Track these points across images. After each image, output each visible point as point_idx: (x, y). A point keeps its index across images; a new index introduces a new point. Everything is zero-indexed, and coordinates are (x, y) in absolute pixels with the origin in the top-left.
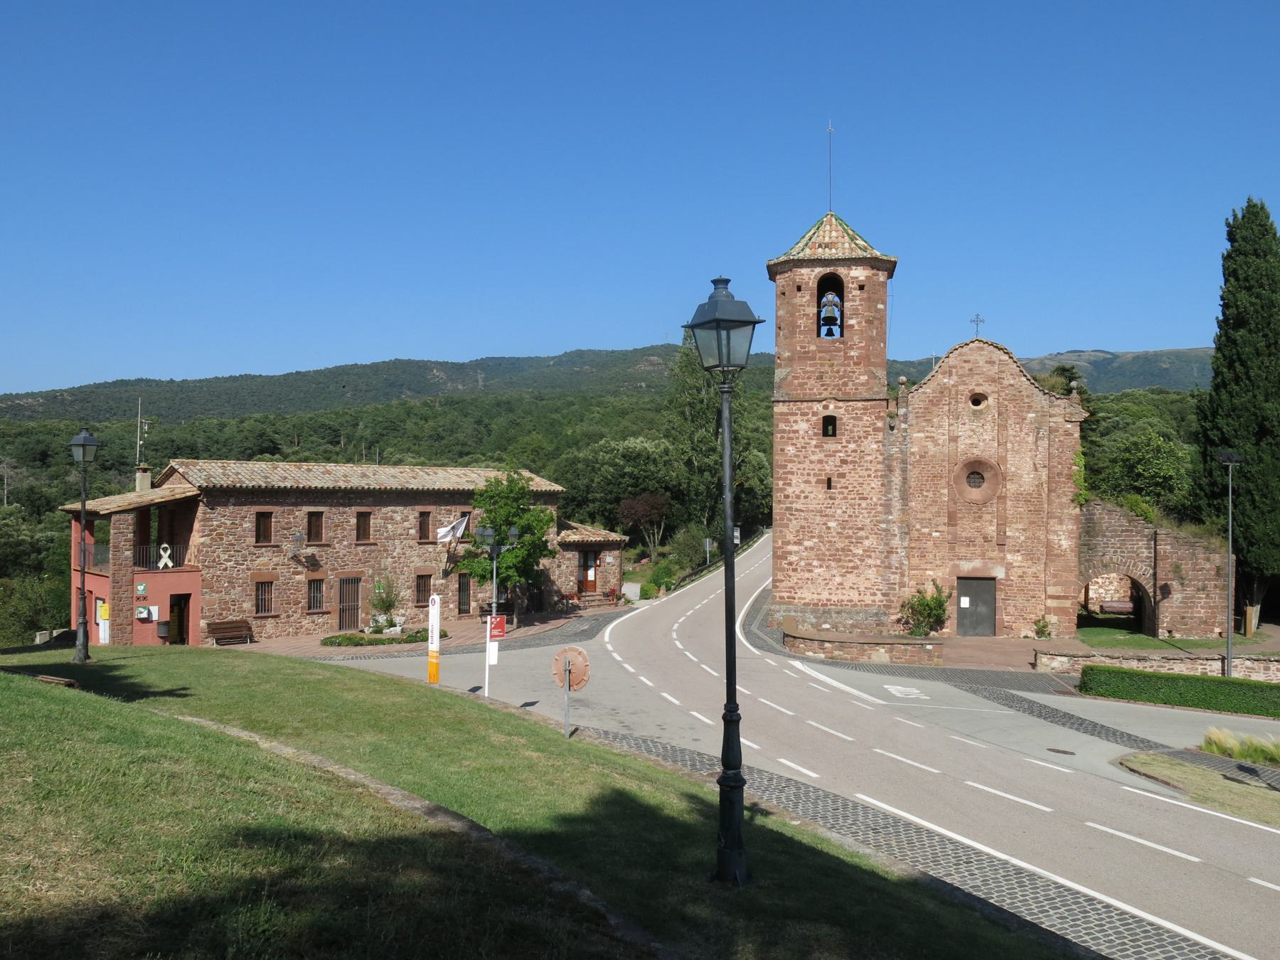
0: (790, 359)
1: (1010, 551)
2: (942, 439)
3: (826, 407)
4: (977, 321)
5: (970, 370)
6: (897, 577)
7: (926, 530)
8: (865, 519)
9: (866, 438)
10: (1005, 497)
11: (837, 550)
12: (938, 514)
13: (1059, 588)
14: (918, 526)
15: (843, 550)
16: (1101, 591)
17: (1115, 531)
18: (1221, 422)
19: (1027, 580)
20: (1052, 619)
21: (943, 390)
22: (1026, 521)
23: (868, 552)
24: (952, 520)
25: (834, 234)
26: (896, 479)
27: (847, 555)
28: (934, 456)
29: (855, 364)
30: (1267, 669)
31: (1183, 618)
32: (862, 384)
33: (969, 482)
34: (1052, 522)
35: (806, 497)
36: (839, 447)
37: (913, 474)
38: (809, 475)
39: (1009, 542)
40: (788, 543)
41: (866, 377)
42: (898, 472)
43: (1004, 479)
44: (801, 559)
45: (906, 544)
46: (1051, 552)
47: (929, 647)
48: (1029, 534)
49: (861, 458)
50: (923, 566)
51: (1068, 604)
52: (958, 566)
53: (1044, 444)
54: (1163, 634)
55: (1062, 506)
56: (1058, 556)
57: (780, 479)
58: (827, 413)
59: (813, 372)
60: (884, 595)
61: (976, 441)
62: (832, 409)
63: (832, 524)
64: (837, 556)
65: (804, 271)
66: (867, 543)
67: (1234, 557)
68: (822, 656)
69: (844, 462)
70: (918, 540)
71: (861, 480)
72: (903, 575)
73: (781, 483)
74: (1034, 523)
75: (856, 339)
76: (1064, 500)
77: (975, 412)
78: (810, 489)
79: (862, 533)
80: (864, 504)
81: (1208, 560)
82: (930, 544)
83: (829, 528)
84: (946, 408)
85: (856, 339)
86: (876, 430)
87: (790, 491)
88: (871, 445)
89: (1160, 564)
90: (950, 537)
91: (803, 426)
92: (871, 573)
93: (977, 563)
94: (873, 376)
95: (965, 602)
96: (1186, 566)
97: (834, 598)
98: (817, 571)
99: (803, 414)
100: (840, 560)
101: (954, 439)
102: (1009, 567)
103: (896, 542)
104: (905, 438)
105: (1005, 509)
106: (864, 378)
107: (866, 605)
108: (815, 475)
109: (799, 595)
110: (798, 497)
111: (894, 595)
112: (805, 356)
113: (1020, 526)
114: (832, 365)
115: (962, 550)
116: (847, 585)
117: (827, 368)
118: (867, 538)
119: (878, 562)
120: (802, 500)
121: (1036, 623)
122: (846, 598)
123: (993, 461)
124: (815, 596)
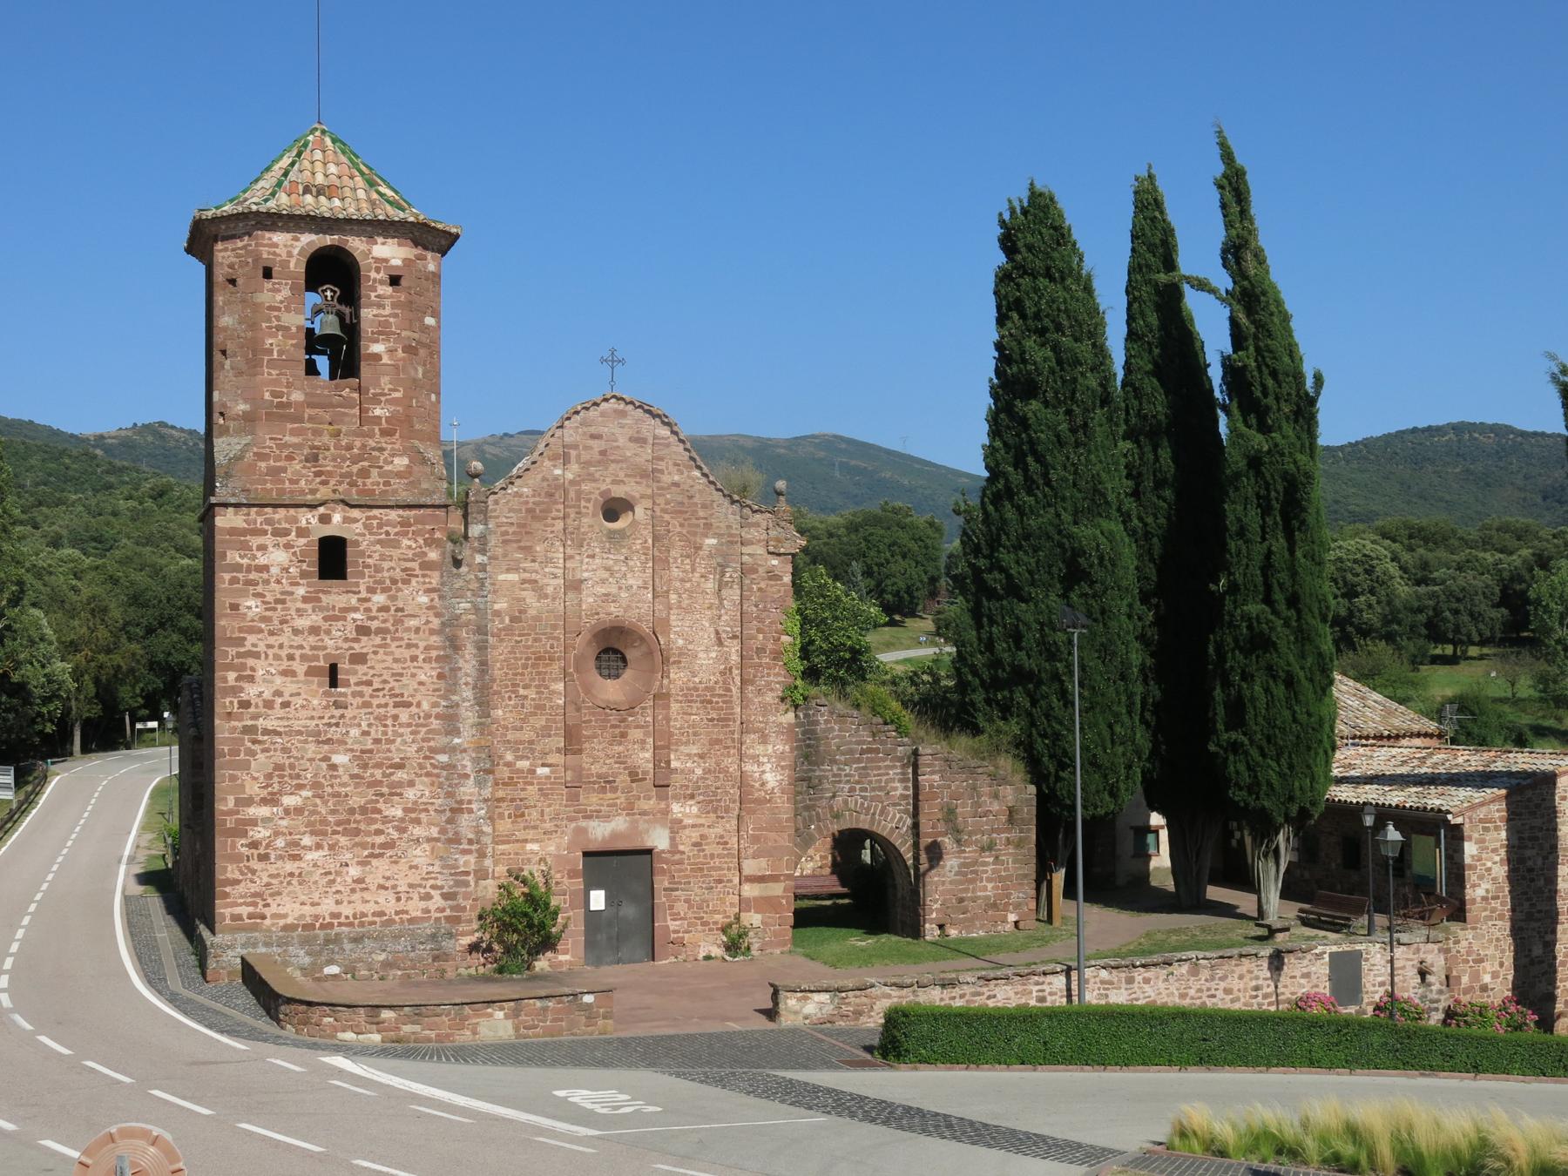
0: (249, 419)
1: (676, 798)
2: (553, 585)
3: (325, 519)
4: (613, 361)
5: (603, 453)
6: (472, 859)
7: (523, 764)
8: (406, 747)
9: (406, 582)
10: (667, 696)
11: (352, 811)
12: (545, 732)
13: (763, 862)
14: (509, 757)
17: (851, 752)
18: (1006, 557)
19: (709, 849)
20: (753, 919)
21: (554, 491)
24: (573, 741)
25: (332, 169)
26: (467, 664)
27: (374, 821)
28: (537, 618)
29: (384, 433)
30: (1130, 981)
31: (961, 900)
32: (399, 475)
33: (599, 668)
34: (748, 739)
35: (286, 705)
37: (499, 652)
38: (291, 657)
39: (677, 781)
40: (249, 802)
41: (405, 461)
42: (469, 651)
43: (665, 661)
44: (277, 834)
45: (487, 793)
46: (747, 796)
47: (588, 999)
48: (710, 763)
49: (398, 622)
50: (520, 835)
51: (777, 889)
52: (584, 831)
53: (733, 594)
54: (931, 931)
55: (765, 709)
57: (230, 667)
58: (328, 531)
59: (294, 446)
60: (445, 896)
61: (614, 590)
62: (338, 523)
63: (340, 759)
64: (351, 824)
65: (279, 238)
66: (411, 794)
67: (1032, 789)
68: (377, 1038)
69: (363, 631)
70: (510, 783)
71: (397, 667)
72: (482, 855)
73: (231, 676)
74: (718, 741)
75: (385, 382)
76: (770, 698)
77: (611, 534)
78: (293, 688)
79: (401, 775)
80: (404, 716)
81: (996, 796)
82: (532, 790)
83: (333, 767)
84: (559, 525)
85: (385, 382)
86: (427, 566)
87: (251, 691)
88: (417, 598)
89: (925, 808)
91: (277, 557)
92: (420, 855)
93: (619, 823)
94: (419, 458)
95: (598, 900)
96: (964, 809)
97: (347, 910)
98: (311, 856)
99: (276, 533)
100: (357, 832)
101: (574, 586)
102: (676, 827)
103: (468, 789)
104: (482, 582)
105: (668, 719)
106: (401, 462)
107: (412, 921)
108: (304, 658)
109: (274, 909)
110: (269, 704)
111: (466, 896)
112: (281, 413)
113: (694, 750)
114: (337, 434)
115: (592, 800)
116: (373, 880)
117: (326, 439)
118: (411, 784)
119: (434, 832)
120: (278, 711)
121: (724, 930)
122: (370, 908)
123: (646, 628)
124: (308, 910)
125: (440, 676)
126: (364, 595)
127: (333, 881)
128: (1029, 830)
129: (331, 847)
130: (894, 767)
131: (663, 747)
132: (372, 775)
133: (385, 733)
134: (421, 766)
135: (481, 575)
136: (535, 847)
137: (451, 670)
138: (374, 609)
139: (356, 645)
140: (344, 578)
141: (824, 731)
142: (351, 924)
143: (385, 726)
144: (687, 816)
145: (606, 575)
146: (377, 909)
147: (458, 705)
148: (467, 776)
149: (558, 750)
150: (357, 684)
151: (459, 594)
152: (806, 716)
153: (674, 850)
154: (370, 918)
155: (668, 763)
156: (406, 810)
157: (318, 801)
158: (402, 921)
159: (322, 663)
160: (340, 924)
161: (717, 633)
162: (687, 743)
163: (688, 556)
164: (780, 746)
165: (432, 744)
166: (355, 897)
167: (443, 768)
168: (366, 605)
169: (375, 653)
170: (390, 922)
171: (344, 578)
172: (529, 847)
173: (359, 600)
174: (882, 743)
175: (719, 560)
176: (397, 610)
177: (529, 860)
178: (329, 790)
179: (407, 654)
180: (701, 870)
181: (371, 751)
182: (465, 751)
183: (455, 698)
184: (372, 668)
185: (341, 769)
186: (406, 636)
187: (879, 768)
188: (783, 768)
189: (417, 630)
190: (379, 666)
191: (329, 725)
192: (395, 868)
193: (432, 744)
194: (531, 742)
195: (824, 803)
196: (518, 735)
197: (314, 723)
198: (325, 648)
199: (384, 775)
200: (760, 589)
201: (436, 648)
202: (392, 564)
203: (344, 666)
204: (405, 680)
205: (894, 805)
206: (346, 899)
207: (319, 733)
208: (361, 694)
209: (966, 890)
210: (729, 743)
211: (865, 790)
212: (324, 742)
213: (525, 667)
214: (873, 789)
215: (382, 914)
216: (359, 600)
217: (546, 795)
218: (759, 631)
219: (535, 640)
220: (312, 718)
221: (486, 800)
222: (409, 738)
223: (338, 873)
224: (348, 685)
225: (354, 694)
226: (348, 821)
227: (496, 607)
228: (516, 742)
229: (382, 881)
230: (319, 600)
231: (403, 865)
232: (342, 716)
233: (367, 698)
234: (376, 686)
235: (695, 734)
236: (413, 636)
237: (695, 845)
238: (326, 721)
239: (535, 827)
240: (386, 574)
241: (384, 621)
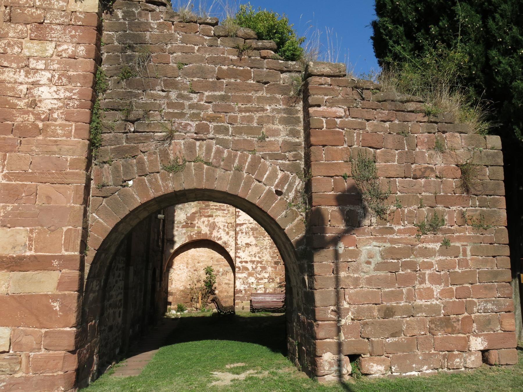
16: (252, 280)
17: (202, 73)
31: (388, 313)
34: (13, 31)
56: (25, 132)
67: (495, 141)
81: (439, 147)
89: (321, 155)
128: (495, 203)
130: (271, 100)
152: (127, 15)
164: (74, 47)
187: (249, 100)
188: (70, 79)
195: (152, 146)
205: (274, 157)
209: (397, 296)
211: (225, 130)
214: (238, 131)
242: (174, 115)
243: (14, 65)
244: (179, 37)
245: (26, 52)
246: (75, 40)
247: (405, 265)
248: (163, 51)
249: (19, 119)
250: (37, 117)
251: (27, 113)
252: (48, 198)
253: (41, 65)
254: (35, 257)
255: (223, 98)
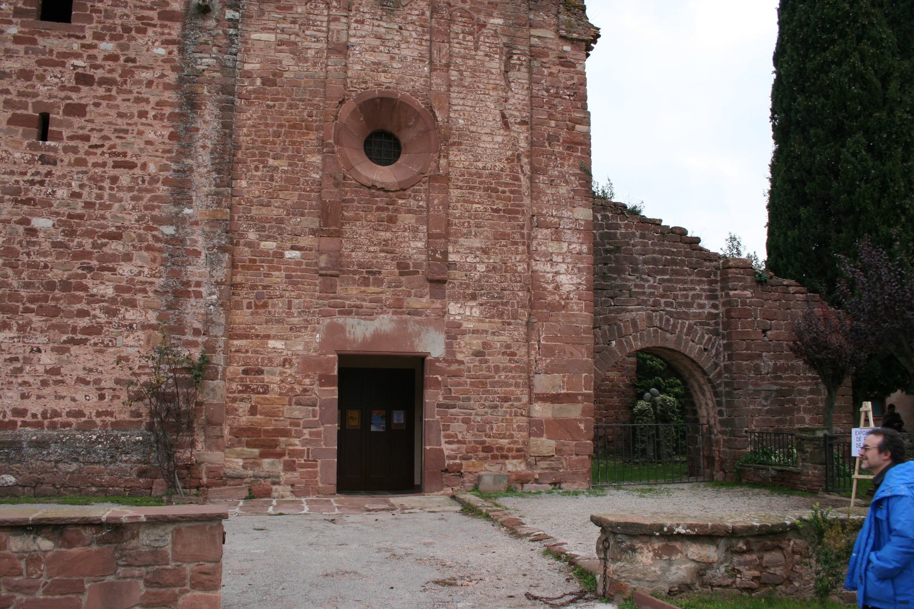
2: (313, 47)
7: (270, 245)
8: (124, 213)
9: (142, 31)
11: (51, 286)
13: (558, 378)
14: (252, 236)
15: (66, 286)
17: (655, 261)
19: (494, 360)
22: (488, 232)
23: (127, 293)
24: (331, 221)
26: (208, 124)
27: (79, 300)
28: (295, 84)
31: (777, 433)
36: (76, 46)
37: (248, 116)
43: (446, 138)
46: (538, 300)
48: (494, 259)
50: (261, 329)
51: (574, 411)
52: (341, 329)
53: (520, 76)
61: (384, 58)
63: (41, 223)
66: (126, 270)
71: (121, 123)
74: (504, 236)
79: (115, 247)
80: (125, 179)
82: (278, 276)
83: (33, 232)
88: (154, 49)
90: (323, 261)
93: (385, 323)
97: (34, 407)
100: (56, 312)
102: (453, 332)
103: (197, 270)
104: (231, 39)
105: (447, 206)
107: (116, 425)
115: (351, 292)
116: (71, 371)
118: (128, 258)
119: (152, 317)
122: (65, 406)
123: (419, 103)
125: (172, 136)
126: (89, 40)
127: (20, 370)
129: (21, 328)
130: (700, 282)
131: (439, 236)
132: (80, 245)
133: (100, 197)
134: (141, 239)
135: (231, 31)
136: (279, 344)
137: (187, 130)
138: (100, 57)
139: (74, 95)
140: (68, 20)
141: (624, 236)
142: (39, 425)
143: (101, 188)
144: (468, 319)
145: (378, 42)
146: (73, 406)
147: (191, 170)
148: (197, 254)
149: (313, 232)
150: (71, 138)
151: (202, 48)
153: (450, 357)
154: (64, 419)
155: (445, 254)
156: (117, 289)
157: (10, 271)
158: (105, 425)
159: (30, 112)
160: (25, 424)
161: (503, 116)
162: (467, 235)
163: (471, 34)
164: (579, 246)
165: (156, 212)
166: (46, 391)
167: (167, 242)
168: (91, 52)
169: (97, 105)
170: (89, 426)
171: (68, 20)
172: (272, 343)
173: (83, 46)
174: (687, 255)
175: (505, 40)
176: (128, 60)
177: (270, 360)
178: (26, 259)
179: (135, 109)
180: (484, 384)
181: (81, 217)
182: (196, 223)
183: (189, 161)
184: (91, 121)
185: (41, 235)
186: (135, 89)
189: (150, 84)
190: (99, 120)
191: (32, 183)
192: (101, 358)
193: (156, 212)
194: (280, 221)
196: (264, 210)
197: (16, 178)
198: (36, 95)
199: (94, 245)
200: (551, 74)
201: (172, 105)
202: (127, 11)
203: (57, 116)
204: (129, 138)
206: (34, 392)
207: (18, 191)
208: (75, 150)
210: (517, 237)
212: (24, 202)
213: (277, 135)
214: (680, 305)
215: (80, 414)
216: (83, 46)
217: (295, 284)
218: (551, 117)
219: (291, 106)
220: (12, 173)
221: (218, 284)
222: (129, 205)
223: (27, 360)
224: (58, 137)
225: (66, 149)
226: (46, 298)
227: (247, 67)
228: (261, 220)
229: (82, 374)
230: (34, 42)
231: (110, 356)
232: (49, 173)
233: (81, 155)
234: (94, 141)
235: (478, 226)
236: (144, 89)
237: (477, 354)
238: (28, 177)
239: (280, 321)
240: (118, 21)
241: (111, 71)
242: (638, 293)
243: (543, 259)
244: (638, 234)
245: (550, 250)
246: (580, 241)
247: (789, 401)
248: (628, 244)
249: (549, 299)
250: (560, 296)
251: (554, 294)
252: (572, 354)
253: (560, 259)
254: (567, 394)
255: (668, 281)
